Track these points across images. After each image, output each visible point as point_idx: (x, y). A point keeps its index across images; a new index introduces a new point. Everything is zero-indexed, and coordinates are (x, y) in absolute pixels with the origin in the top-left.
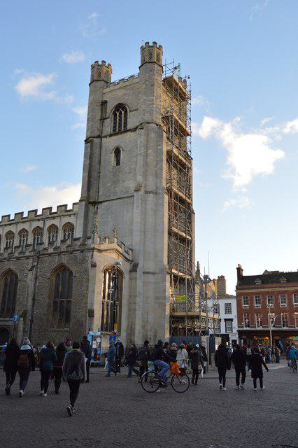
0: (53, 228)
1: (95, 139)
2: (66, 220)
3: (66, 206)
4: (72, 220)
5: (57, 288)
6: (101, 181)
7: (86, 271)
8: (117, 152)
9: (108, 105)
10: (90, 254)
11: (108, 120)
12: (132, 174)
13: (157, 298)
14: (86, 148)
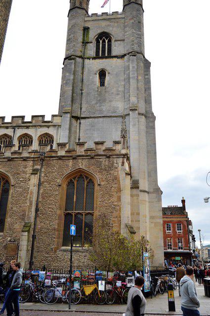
1: (77, 58)
4: (51, 131)
5: (69, 197)
6: (84, 99)
7: (116, 179)
8: (102, 74)
10: (121, 160)
11: (91, 44)
12: (120, 96)
13: (152, 217)
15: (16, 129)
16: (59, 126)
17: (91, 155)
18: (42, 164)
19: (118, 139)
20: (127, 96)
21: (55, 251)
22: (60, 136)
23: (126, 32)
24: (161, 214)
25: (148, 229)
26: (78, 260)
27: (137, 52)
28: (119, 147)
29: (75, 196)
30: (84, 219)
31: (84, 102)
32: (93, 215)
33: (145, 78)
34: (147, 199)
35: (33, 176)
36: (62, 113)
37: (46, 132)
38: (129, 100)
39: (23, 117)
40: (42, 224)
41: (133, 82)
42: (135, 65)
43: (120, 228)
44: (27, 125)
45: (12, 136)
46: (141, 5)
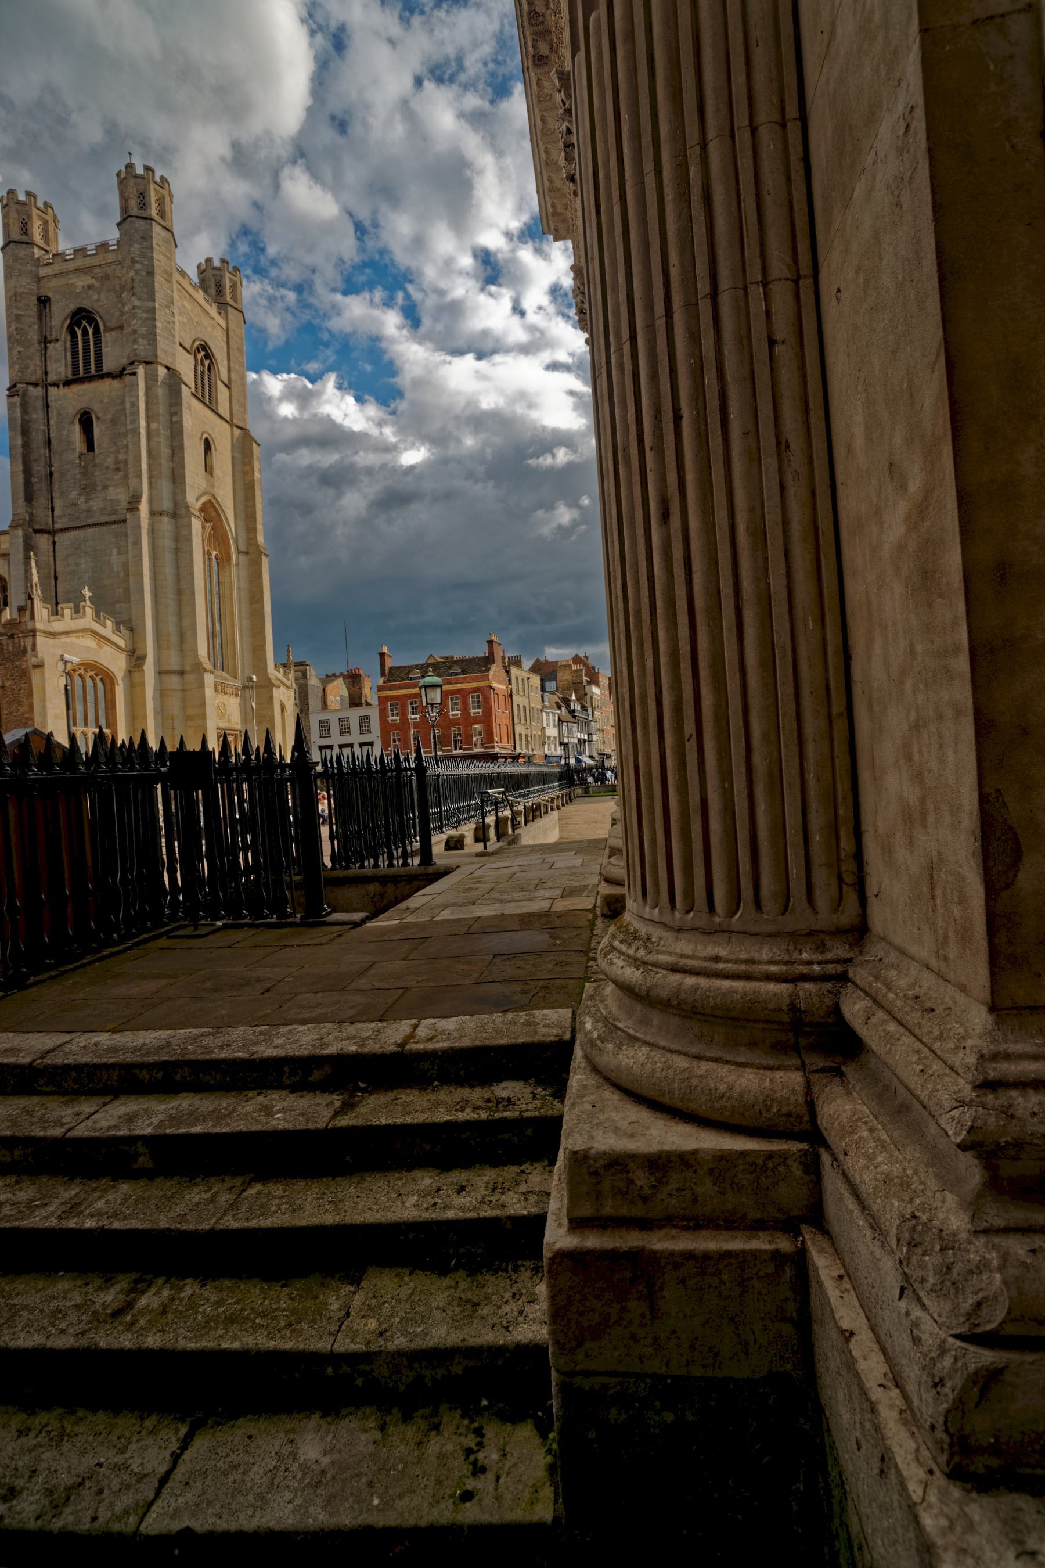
1: (31, 388)
6: (56, 486)
7: (24, 675)
8: (86, 421)
9: (54, 308)
10: (30, 639)
11: (58, 345)
14: (11, 407)
31: (56, 494)
33: (171, 422)
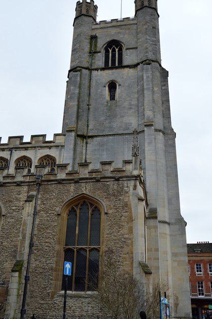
0: (24, 162)
1: (83, 70)
2: (46, 152)
3: (44, 136)
4: (53, 153)
7: (126, 205)
8: (112, 86)
9: (99, 40)
10: (132, 183)
11: (99, 54)
13: (174, 255)
15: (14, 151)
16: (62, 146)
17: (97, 179)
18: (39, 189)
19: (129, 156)
20: (141, 110)
21: (53, 297)
22: (63, 157)
23: (139, 39)
24: (185, 250)
25: (170, 270)
26: (80, 307)
27: (153, 61)
28: (129, 167)
29: (77, 228)
30: (88, 256)
31: (91, 118)
32: (99, 251)
34: (168, 232)
35: (27, 204)
36: (67, 130)
37: (46, 154)
38: (144, 115)
39: (21, 138)
40: (37, 263)
41: (147, 94)
42: (149, 75)
43: (132, 267)
44: (25, 146)
45: (9, 159)
46: (156, 9)
